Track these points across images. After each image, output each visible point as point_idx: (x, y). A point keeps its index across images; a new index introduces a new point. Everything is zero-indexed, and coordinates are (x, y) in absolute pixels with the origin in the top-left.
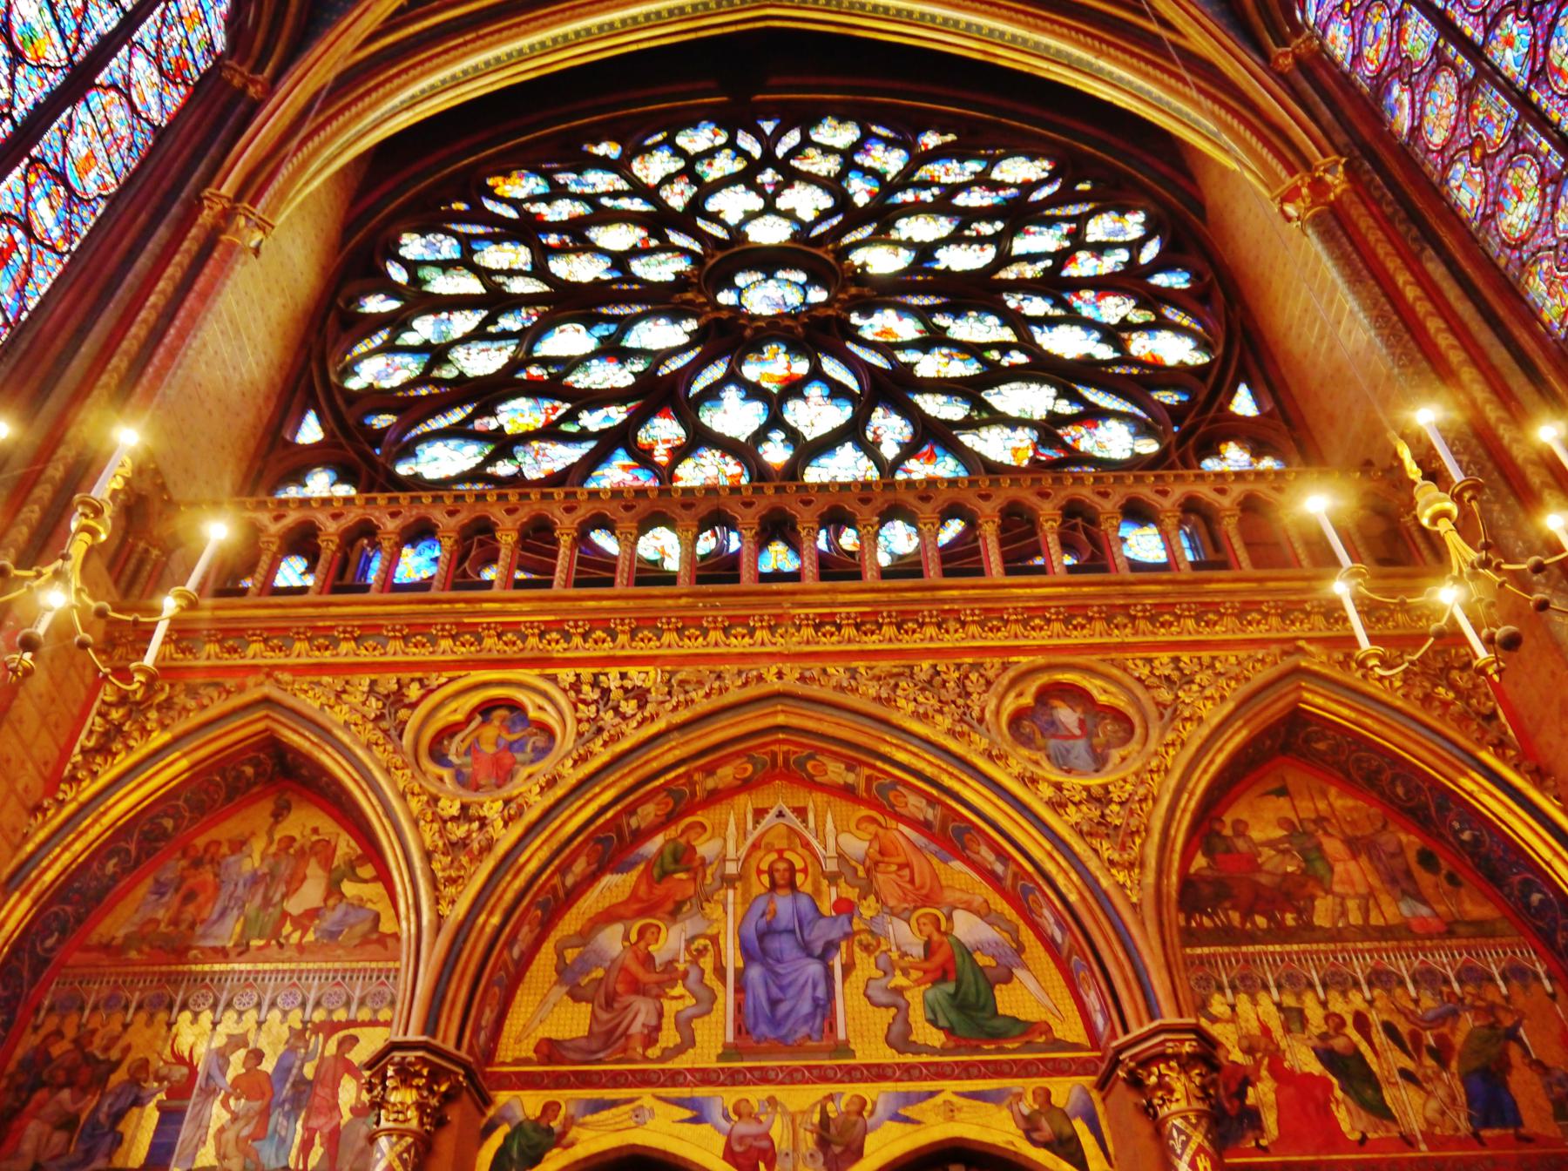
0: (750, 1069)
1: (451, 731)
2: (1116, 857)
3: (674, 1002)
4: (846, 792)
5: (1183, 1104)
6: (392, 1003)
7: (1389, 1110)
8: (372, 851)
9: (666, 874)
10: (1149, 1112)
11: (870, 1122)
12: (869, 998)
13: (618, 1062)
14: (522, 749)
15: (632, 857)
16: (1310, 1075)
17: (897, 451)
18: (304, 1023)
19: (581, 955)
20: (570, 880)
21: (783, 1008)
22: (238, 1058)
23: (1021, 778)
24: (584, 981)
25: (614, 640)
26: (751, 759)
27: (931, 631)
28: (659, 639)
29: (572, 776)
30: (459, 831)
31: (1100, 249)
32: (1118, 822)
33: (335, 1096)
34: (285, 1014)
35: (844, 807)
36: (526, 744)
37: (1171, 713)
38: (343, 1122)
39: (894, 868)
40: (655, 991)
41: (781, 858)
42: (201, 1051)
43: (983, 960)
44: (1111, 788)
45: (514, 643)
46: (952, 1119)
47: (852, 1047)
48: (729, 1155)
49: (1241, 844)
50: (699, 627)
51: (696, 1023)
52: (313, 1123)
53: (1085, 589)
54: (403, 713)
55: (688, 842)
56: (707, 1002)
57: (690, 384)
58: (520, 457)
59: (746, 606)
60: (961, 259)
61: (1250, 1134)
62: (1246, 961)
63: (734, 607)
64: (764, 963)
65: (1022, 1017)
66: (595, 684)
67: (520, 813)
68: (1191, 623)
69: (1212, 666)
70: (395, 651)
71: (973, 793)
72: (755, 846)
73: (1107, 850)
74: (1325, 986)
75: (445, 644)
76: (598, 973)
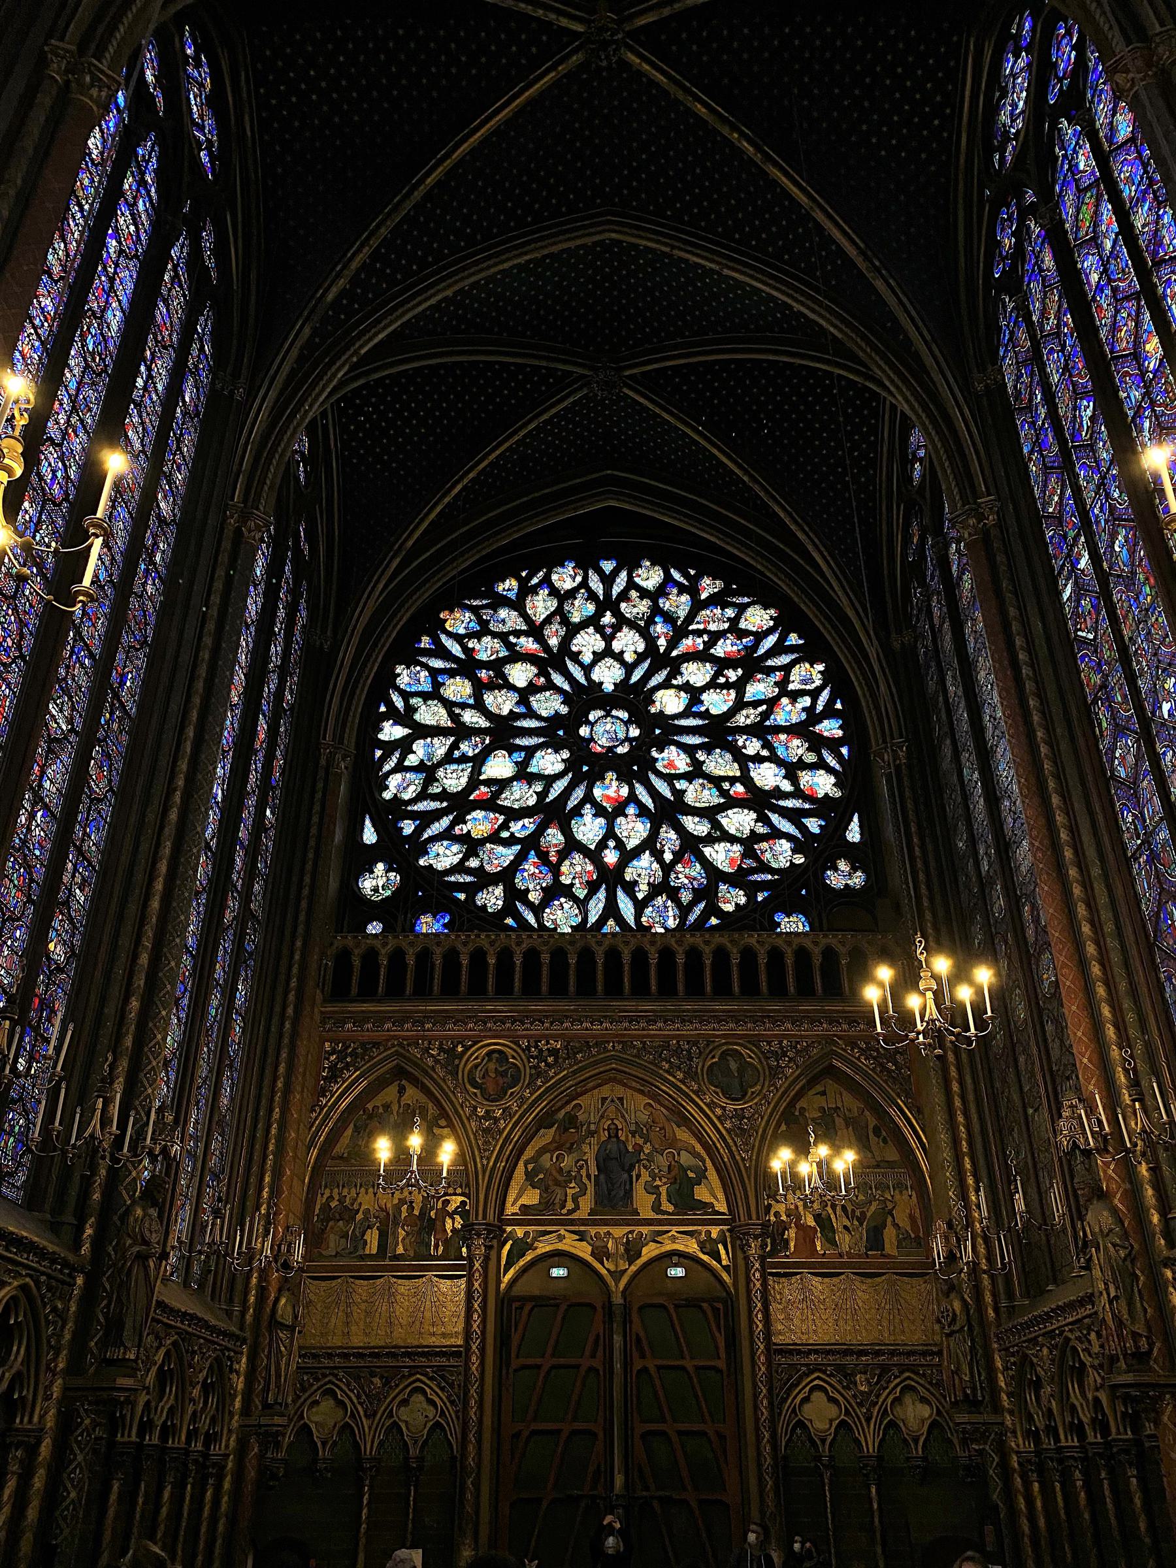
1: (476, 1066)
4: (641, 1092)
9: (566, 1130)
17: (671, 857)
21: (613, 1193)
31: (795, 696)
37: (775, 1072)
42: (389, 1205)
43: (691, 1175)
56: (583, 1192)
57: (566, 804)
58: (481, 853)
60: (717, 702)
66: (536, 1047)
72: (602, 1117)
76: (541, 1176)
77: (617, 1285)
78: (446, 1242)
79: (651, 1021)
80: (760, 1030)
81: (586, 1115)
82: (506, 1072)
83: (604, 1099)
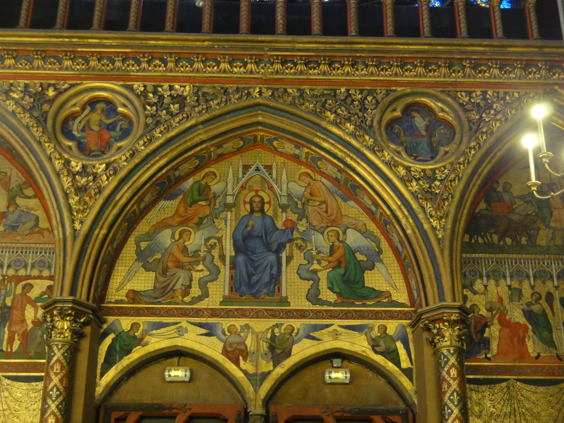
0: (236, 310)
2: (433, 213)
3: (198, 273)
4: (295, 158)
5: (448, 343)
6: (49, 267)
7: (554, 342)
8: (31, 181)
9: (194, 202)
10: (432, 343)
11: (295, 338)
14: (114, 129)
16: (518, 323)
19: (149, 246)
20: (142, 205)
21: (255, 278)
25: (165, 66)
26: (242, 139)
27: (347, 69)
28: (191, 67)
29: (144, 151)
30: (83, 181)
32: (437, 191)
33: (23, 315)
35: (292, 165)
36: (116, 126)
38: (29, 329)
39: (317, 203)
40: (189, 267)
41: (257, 195)
43: (360, 257)
44: (437, 172)
45: (108, 65)
46: (336, 339)
47: (289, 300)
49: (506, 197)
50: (215, 60)
51: (210, 285)
52: (13, 329)
53: (439, 48)
54: (46, 107)
55: (207, 183)
56: (215, 274)
59: (243, 49)
61: (483, 352)
62: (497, 263)
63: (235, 49)
64: (246, 254)
65: (377, 289)
66: (155, 92)
67: (116, 172)
68: (496, 72)
69: (504, 98)
71: (362, 169)
72: (243, 188)
73: (429, 207)
74: (535, 277)
75: (68, 63)
76: (158, 256)
77: (256, 391)
78: (25, 337)
81: (221, 186)
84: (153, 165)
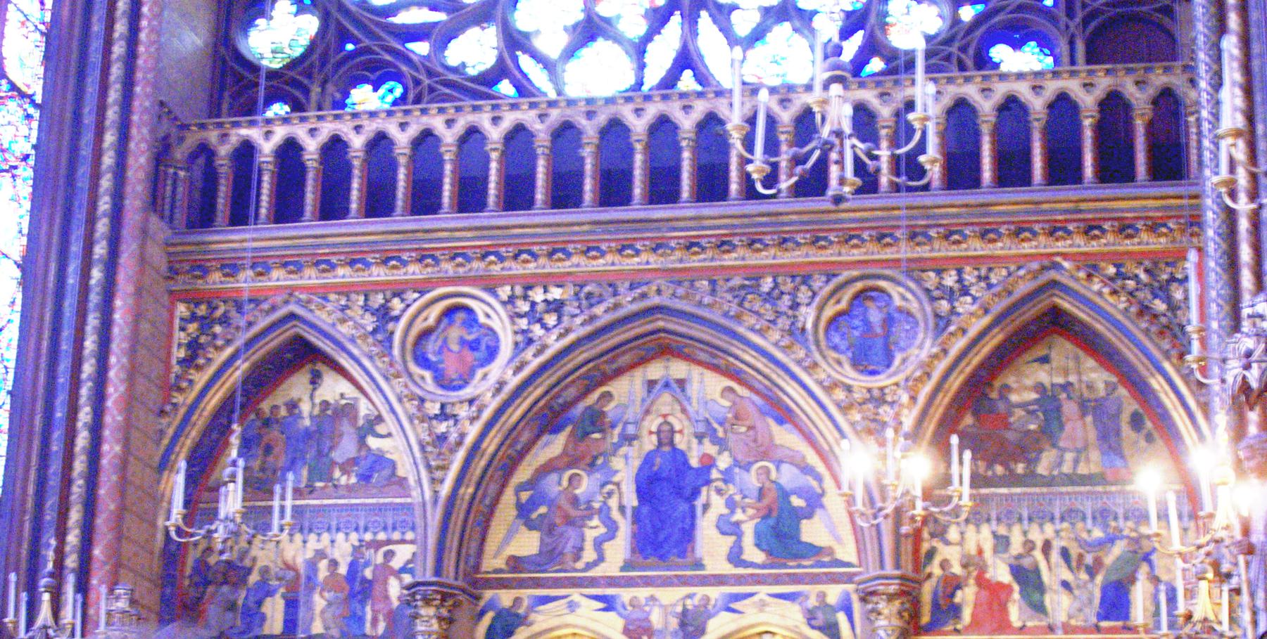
4: (715, 368)
12: (718, 527)
13: (557, 571)
15: (561, 420)
18: (360, 541)
19: (532, 496)
20: (519, 447)
21: (662, 537)
22: (323, 565)
23: (820, 383)
24: (534, 515)
29: (514, 382)
30: (442, 428)
33: (386, 591)
34: (347, 534)
43: (797, 502)
44: (887, 391)
46: (761, 611)
48: (626, 631)
49: (1001, 406)
52: (376, 607)
54: (390, 326)
56: (612, 529)
66: (525, 297)
67: (480, 411)
70: (379, 274)
71: (792, 389)
76: (543, 510)
79: (724, 245)
80: (923, 252)
82: (477, 341)
83: (651, 384)
84: (526, 398)
